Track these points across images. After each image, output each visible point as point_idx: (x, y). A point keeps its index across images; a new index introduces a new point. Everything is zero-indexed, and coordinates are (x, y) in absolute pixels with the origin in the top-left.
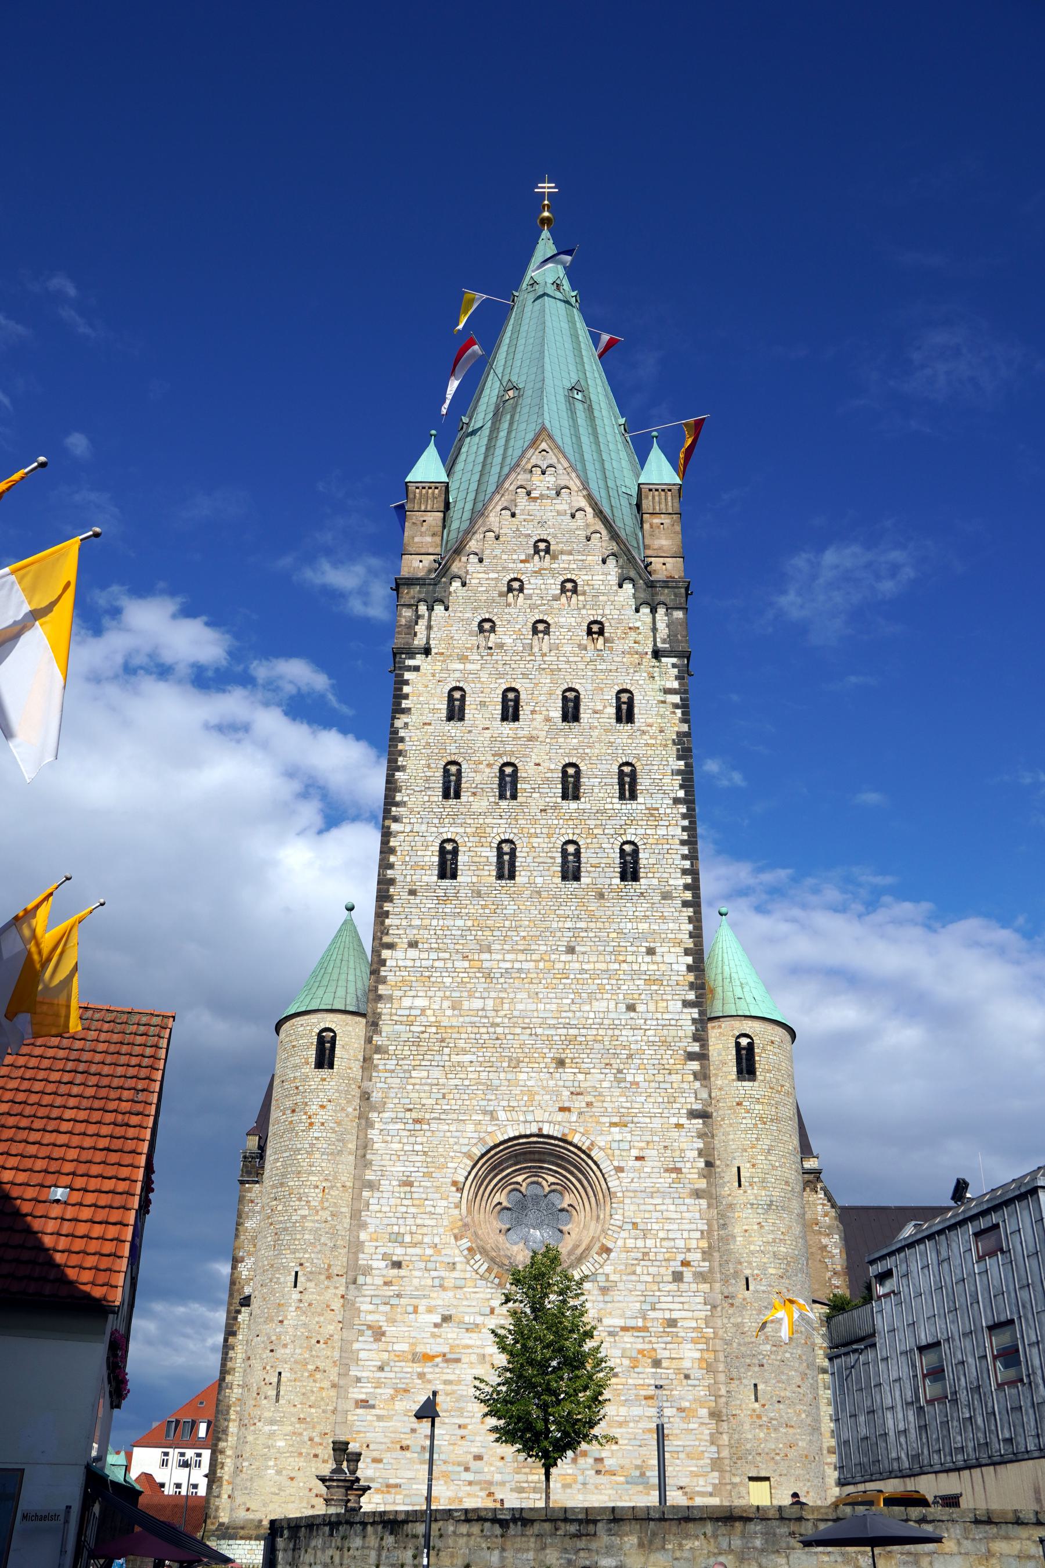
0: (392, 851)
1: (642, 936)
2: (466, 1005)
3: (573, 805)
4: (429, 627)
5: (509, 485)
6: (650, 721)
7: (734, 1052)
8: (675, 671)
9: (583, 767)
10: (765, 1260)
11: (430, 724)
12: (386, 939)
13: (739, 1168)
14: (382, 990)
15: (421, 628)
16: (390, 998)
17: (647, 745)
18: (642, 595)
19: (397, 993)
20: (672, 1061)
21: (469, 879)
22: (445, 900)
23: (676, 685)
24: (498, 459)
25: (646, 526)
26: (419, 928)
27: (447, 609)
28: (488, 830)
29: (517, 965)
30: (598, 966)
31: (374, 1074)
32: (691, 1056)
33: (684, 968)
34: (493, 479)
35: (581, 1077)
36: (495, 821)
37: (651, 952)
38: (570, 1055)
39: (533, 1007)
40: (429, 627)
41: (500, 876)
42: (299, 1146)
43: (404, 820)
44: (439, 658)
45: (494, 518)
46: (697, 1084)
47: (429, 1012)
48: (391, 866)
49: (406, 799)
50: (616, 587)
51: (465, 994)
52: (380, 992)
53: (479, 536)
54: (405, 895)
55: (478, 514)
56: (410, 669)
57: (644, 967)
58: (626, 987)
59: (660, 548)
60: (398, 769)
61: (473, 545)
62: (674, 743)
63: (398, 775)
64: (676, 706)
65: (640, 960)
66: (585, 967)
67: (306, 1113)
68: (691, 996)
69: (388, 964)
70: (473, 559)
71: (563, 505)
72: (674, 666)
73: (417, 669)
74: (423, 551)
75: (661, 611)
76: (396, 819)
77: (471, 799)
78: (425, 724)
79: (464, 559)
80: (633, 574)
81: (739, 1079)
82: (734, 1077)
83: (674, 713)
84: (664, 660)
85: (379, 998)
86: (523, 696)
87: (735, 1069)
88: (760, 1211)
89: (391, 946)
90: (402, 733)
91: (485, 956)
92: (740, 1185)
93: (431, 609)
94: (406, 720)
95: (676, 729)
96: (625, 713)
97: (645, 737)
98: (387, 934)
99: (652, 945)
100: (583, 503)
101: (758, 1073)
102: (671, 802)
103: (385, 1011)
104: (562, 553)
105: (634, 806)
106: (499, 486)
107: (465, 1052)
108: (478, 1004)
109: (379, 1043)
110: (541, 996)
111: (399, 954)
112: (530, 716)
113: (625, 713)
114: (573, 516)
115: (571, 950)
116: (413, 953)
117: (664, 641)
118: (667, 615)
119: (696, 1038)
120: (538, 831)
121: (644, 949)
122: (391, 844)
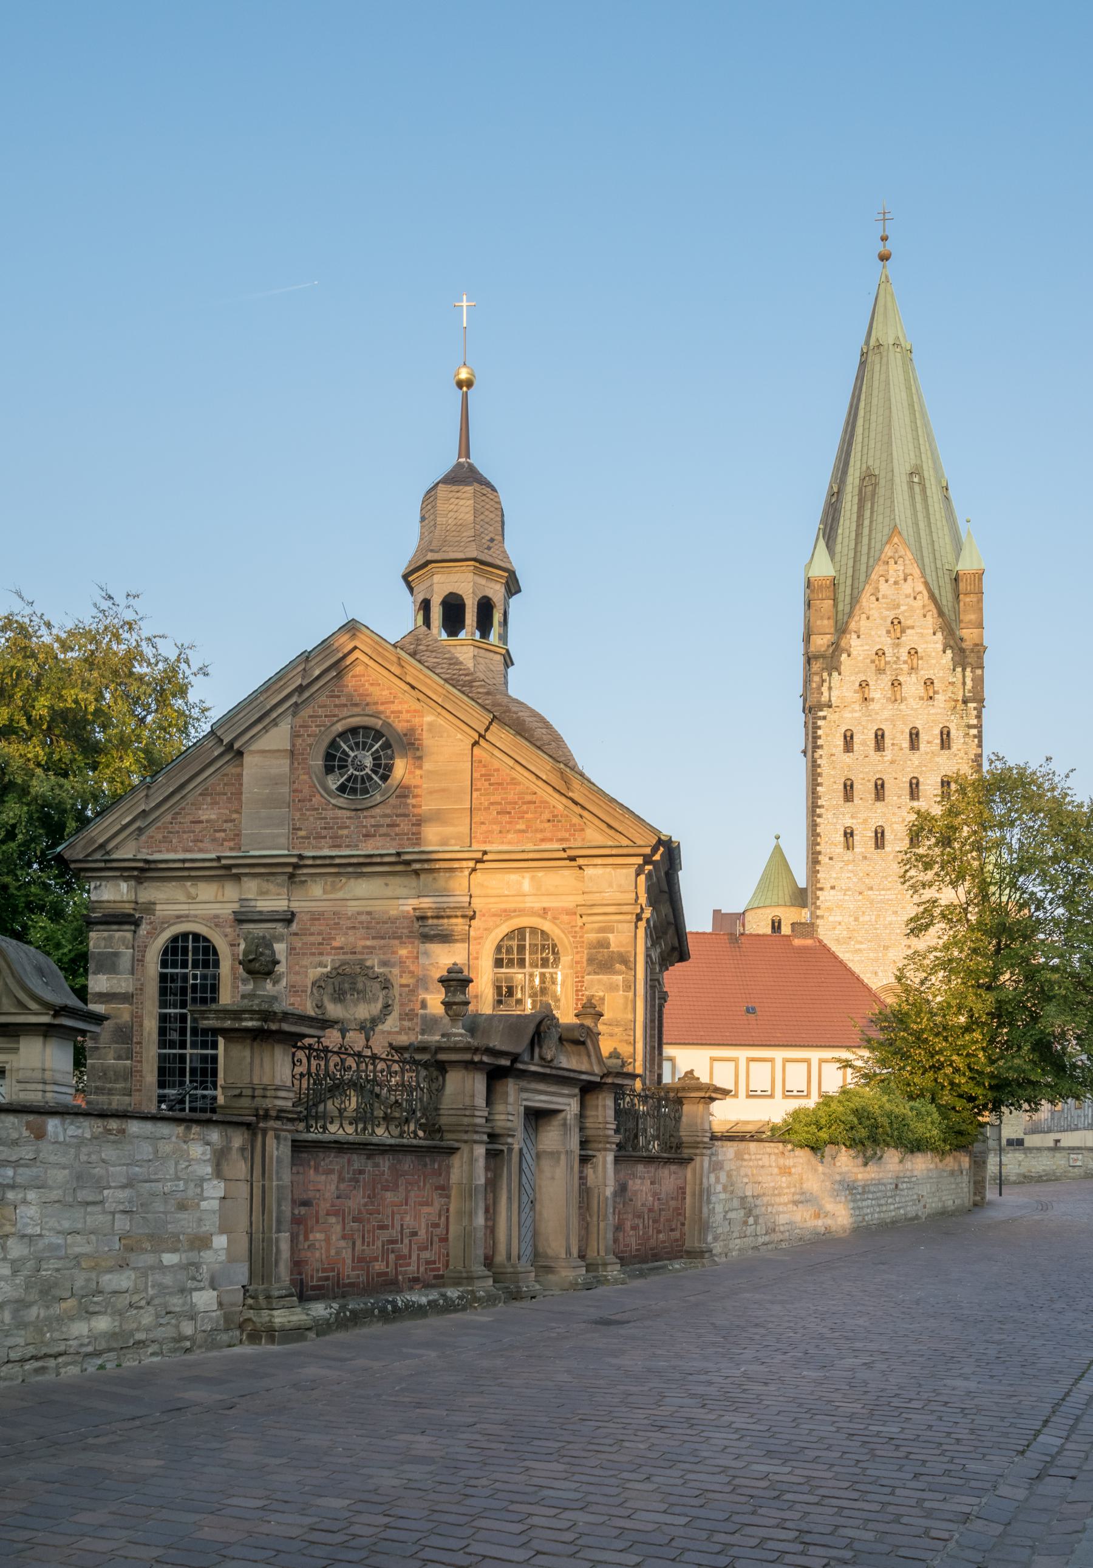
0: (819, 835)
2: (861, 919)
4: (830, 688)
5: (874, 576)
9: (921, 780)
12: (819, 886)
14: (819, 912)
15: (825, 689)
16: (822, 917)
18: (957, 659)
19: (826, 914)
22: (847, 863)
23: (975, 722)
24: (865, 549)
25: (962, 604)
34: (863, 568)
40: (830, 688)
44: (837, 709)
45: (867, 600)
48: (818, 844)
53: (856, 618)
54: (827, 860)
55: (855, 601)
56: (820, 718)
59: (970, 622)
60: (819, 785)
61: (853, 625)
63: (819, 788)
64: (975, 736)
70: (854, 636)
71: (907, 588)
72: (975, 709)
73: (824, 718)
74: (822, 631)
75: (969, 670)
76: (819, 816)
80: (952, 643)
84: (970, 705)
86: (886, 734)
89: (821, 889)
90: (819, 761)
91: (870, 892)
93: (830, 675)
96: (945, 739)
100: (921, 587)
104: (908, 628)
106: (868, 576)
107: (861, 943)
108: (867, 918)
113: (945, 739)
114: (915, 598)
116: (832, 892)
117: (970, 692)
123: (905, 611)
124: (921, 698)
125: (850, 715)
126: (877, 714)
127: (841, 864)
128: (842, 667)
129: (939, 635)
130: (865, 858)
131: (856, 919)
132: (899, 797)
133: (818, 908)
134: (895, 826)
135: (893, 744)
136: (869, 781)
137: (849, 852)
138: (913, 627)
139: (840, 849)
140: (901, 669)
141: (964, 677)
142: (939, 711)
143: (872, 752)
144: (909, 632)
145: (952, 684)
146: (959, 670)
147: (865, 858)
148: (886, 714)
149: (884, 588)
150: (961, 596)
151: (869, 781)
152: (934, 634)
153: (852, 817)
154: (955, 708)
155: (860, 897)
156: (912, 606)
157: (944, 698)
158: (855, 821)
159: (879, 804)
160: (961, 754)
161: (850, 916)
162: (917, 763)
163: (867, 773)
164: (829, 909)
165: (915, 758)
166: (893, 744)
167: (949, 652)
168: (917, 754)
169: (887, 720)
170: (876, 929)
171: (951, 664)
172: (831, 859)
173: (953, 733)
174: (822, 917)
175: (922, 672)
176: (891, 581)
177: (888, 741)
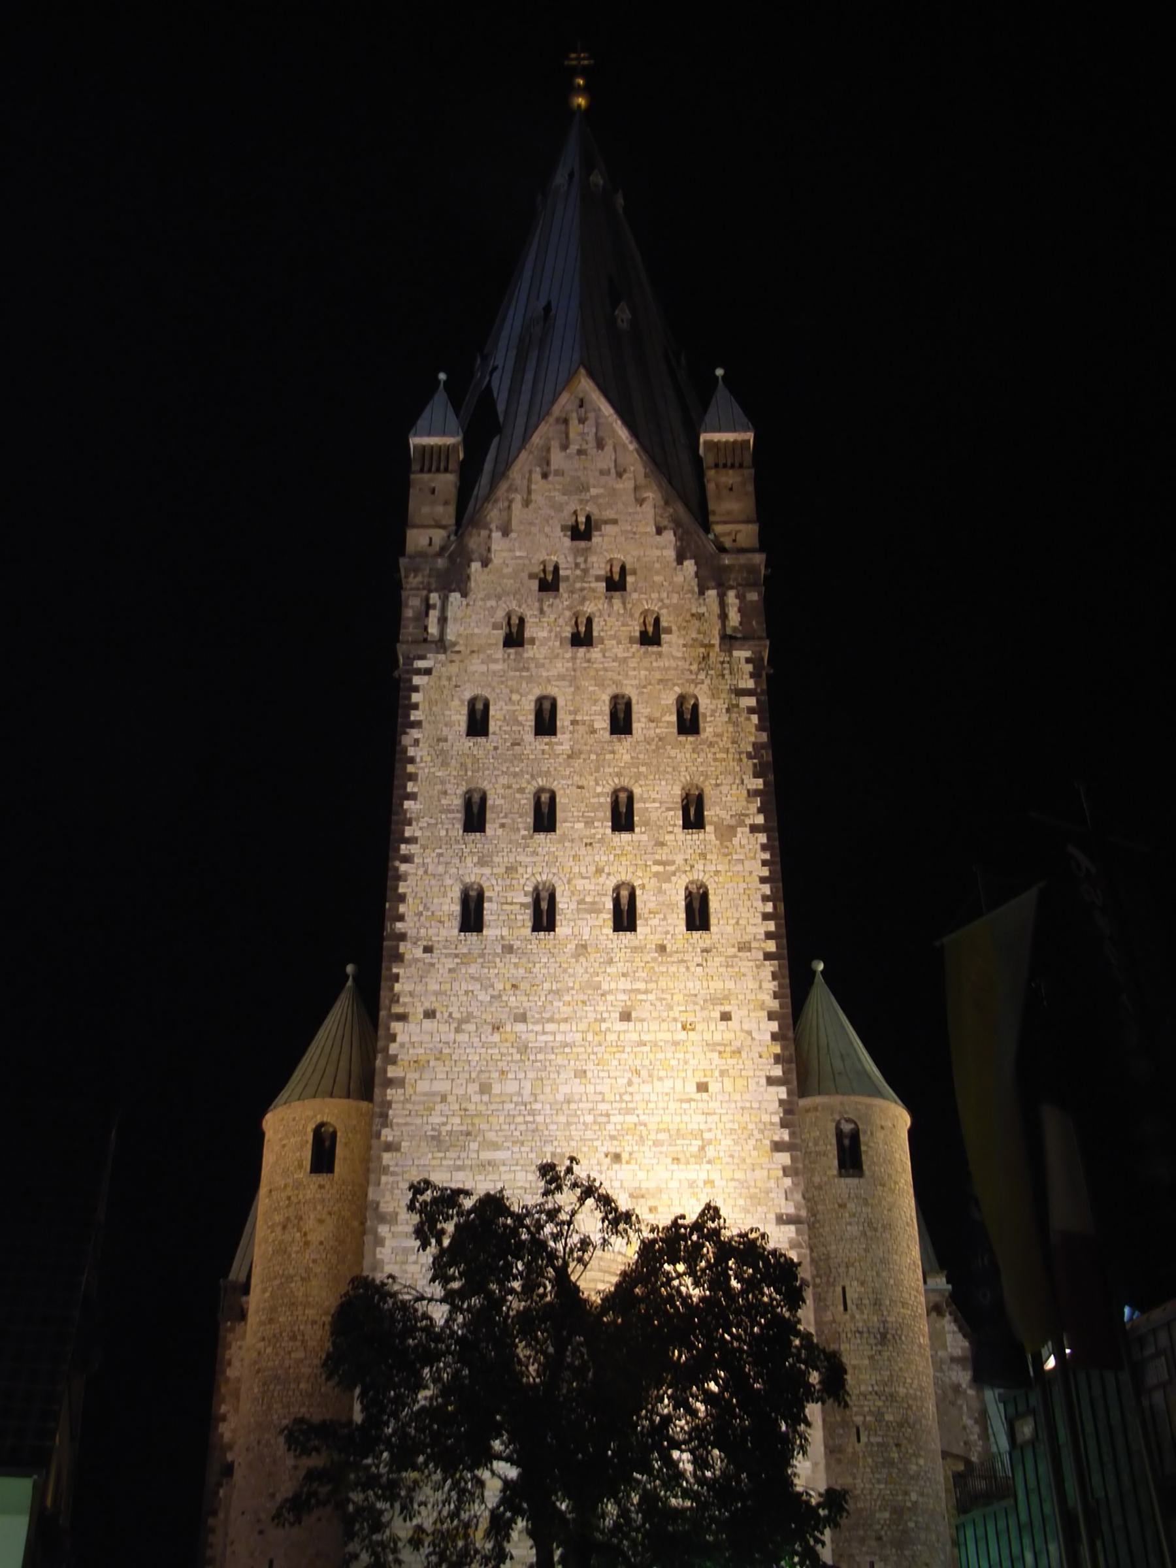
1: (714, 1000)
2: (496, 1089)
3: (625, 837)
4: (443, 620)
6: (719, 730)
7: (834, 1141)
8: (750, 667)
9: (637, 791)
10: (880, 1403)
11: (446, 740)
12: (397, 1009)
13: (844, 1289)
16: (400, 1083)
17: (715, 760)
19: (411, 1076)
20: (754, 1153)
21: (498, 932)
22: (466, 959)
23: (750, 684)
26: (437, 994)
27: (464, 595)
28: (521, 870)
29: (559, 1038)
30: (660, 1036)
31: (384, 1179)
32: (778, 1147)
33: (769, 1037)
35: (641, 1175)
36: (529, 859)
37: (726, 1017)
38: (628, 1149)
39: (582, 1089)
41: (537, 928)
42: (291, 1272)
43: (416, 860)
46: (788, 1182)
47: (450, 1098)
49: (418, 834)
50: (675, 564)
51: (495, 1075)
52: (390, 1075)
53: (502, 504)
54: (418, 953)
56: (419, 672)
57: (718, 1037)
58: (695, 1062)
59: (729, 513)
62: (749, 756)
65: (713, 1027)
66: (645, 1038)
67: (299, 1230)
68: (777, 1071)
69: (398, 1039)
72: (748, 661)
73: (428, 672)
77: (500, 832)
78: (439, 740)
79: (484, 533)
81: (840, 1175)
82: (835, 1172)
83: (749, 719)
84: (736, 653)
85: (390, 1083)
86: (561, 703)
87: (836, 1162)
88: (872, 1341)
89: (402, 1018)
91: (520, 1027)
92: (846, 1309)
94: (417, 736)
95: (752, 739)
97: (713, 750)
98: (398, 1001)
99: (727, 1008)
101: (865, 1167)
102: (748, 829)
103: (396, 1098)
104: (606, 522)
105: (702, 836)
109: (390, 1139)
110: (589, 1074)
111: (412, 1027)
112: (571, 728)
115: (626, 1017)
116: (428, 1024)
118: (737, 597)
119: (784, 1125)
120: (583, 870)
121: (718, 1015)
122: (401, 890)
123: (598, 496)
124: (632, 640)
125: (484, 668)
126: (543, 665)
127: (450, 963)
128: (473, 584)
129: (669, 536)
130: (509, 949)
131: (485, 1089)
132: (589, 823)
133: (393, 1060)
134: (580, 884)
135: (574, 723)
136: (521, 790)
137: (472, 937)
138: (614, 522)
139: (452, 930)
140: (593, 590)
141: (723, 605)
142: (673, 664)
143: (529, 736)
144: (608, 529)
145: (699, 617)
146: (712, 593)
147: (509, 949)
148: (560, 667)
149: (557, 459)
150: (711, 474)
151: (521, 790)
152: (659, 531)
153: (482, 863)
154: (705, 658)
155: (496, 1038)
156: (614, 490)
157: (682, 642)
158: (487, 871)
159: (541, 837)
160: (725, 742)
161: (470, 1080)
162: (627, 757)
163: (515, 775)
164: (418, 1065)
165: (624, 748)
166: (574, 723)
167: (690, 566)
168: (628, 741)
169: (561, 677)
170: (532, 1113)
171: (694, 582)
172: (428, 950)
173: (705, 704)
174: (400, 1083)
175: (635, 596)
176: (574, 448)
177: (563, 719)
